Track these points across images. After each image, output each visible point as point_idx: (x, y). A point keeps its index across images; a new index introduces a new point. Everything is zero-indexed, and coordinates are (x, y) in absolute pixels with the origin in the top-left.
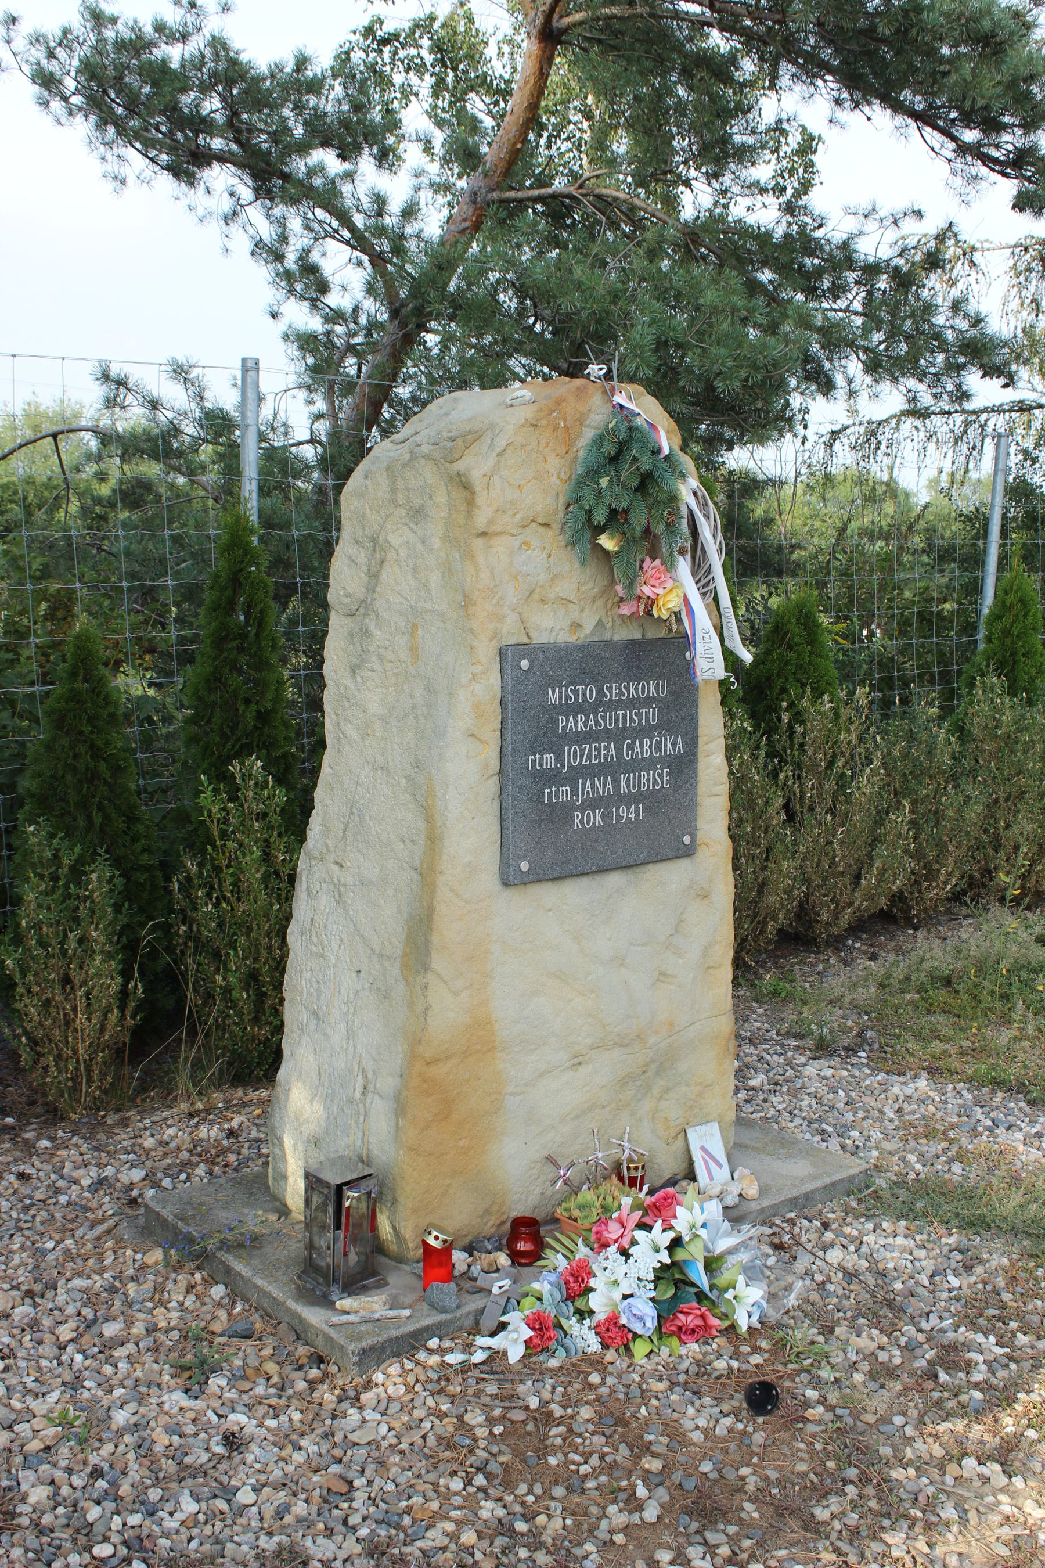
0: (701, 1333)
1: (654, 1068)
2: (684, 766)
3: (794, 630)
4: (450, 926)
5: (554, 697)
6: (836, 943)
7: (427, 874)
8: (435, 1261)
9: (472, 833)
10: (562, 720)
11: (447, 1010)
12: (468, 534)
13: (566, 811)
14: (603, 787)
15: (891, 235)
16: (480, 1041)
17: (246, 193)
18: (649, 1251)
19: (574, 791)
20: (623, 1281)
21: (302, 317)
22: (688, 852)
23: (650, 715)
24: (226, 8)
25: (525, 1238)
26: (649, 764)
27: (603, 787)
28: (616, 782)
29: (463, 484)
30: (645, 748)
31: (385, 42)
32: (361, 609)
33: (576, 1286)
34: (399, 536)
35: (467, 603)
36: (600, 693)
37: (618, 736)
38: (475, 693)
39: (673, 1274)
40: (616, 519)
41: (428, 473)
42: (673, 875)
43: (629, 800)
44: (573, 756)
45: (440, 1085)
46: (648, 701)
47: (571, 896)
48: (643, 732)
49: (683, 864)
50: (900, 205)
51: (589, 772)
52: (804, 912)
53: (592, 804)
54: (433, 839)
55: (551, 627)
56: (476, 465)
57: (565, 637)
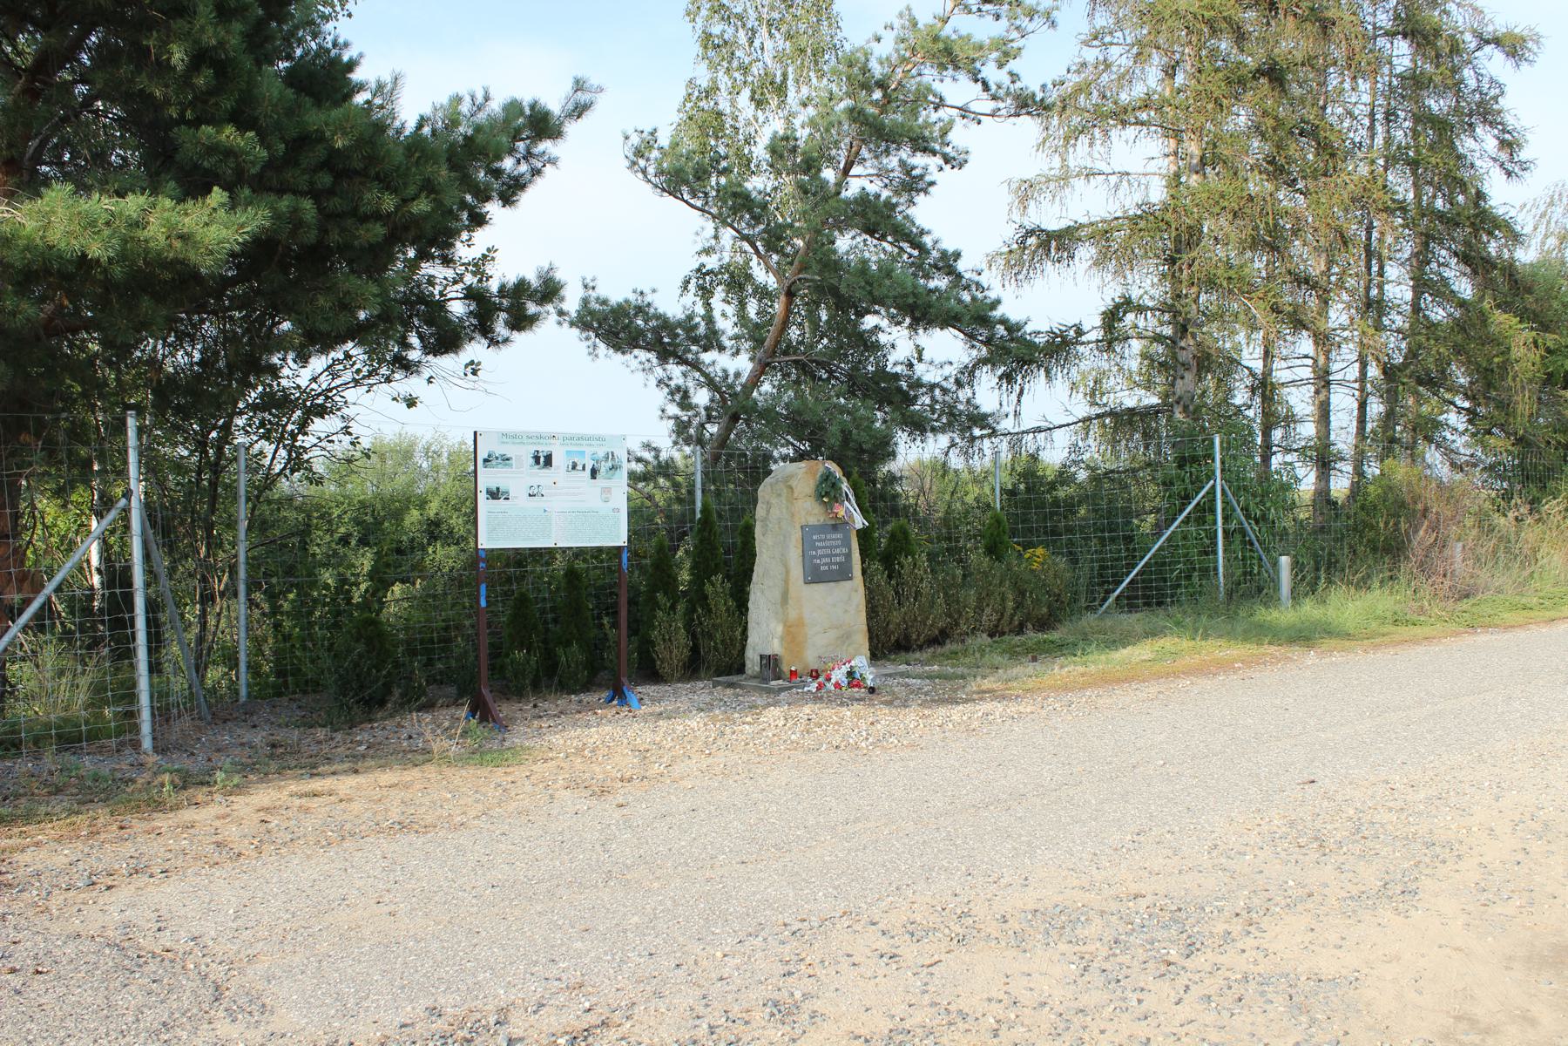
0: (858, 686)
1: (846, 637)
2: (848, 556)
3: (900, 536)
4: (792, 593)
6: (920, 648)
7: (786, 581)
8: (794, 674)
9: (797, 572)
11: (793, 614)
12: (792, 498)
14: (827, 560)
15: (940, 372)
16: (800, 623)
17: (655, 361)
18: (845, 669)
20: (839, 675)
21: (673, 410)
24: (654, 291)
25: (815, 675)
27: (827, 560)
29: (791, 488)
31: (708, 273)
32: (765, 520)
33: (829, 679)
34: (774, 501)
35: (793, 515)
37: (830, 547)
38: (796, 535)
39: (850, 674)
40: (827, 494)
41: (781, 485)
42: (847, 584)
45: (793, 634)
47: (820, 588)
50: (943, 359)
52: (907, 637)
54: (787, 572)
55: (813, 521)
56: (794, 483)
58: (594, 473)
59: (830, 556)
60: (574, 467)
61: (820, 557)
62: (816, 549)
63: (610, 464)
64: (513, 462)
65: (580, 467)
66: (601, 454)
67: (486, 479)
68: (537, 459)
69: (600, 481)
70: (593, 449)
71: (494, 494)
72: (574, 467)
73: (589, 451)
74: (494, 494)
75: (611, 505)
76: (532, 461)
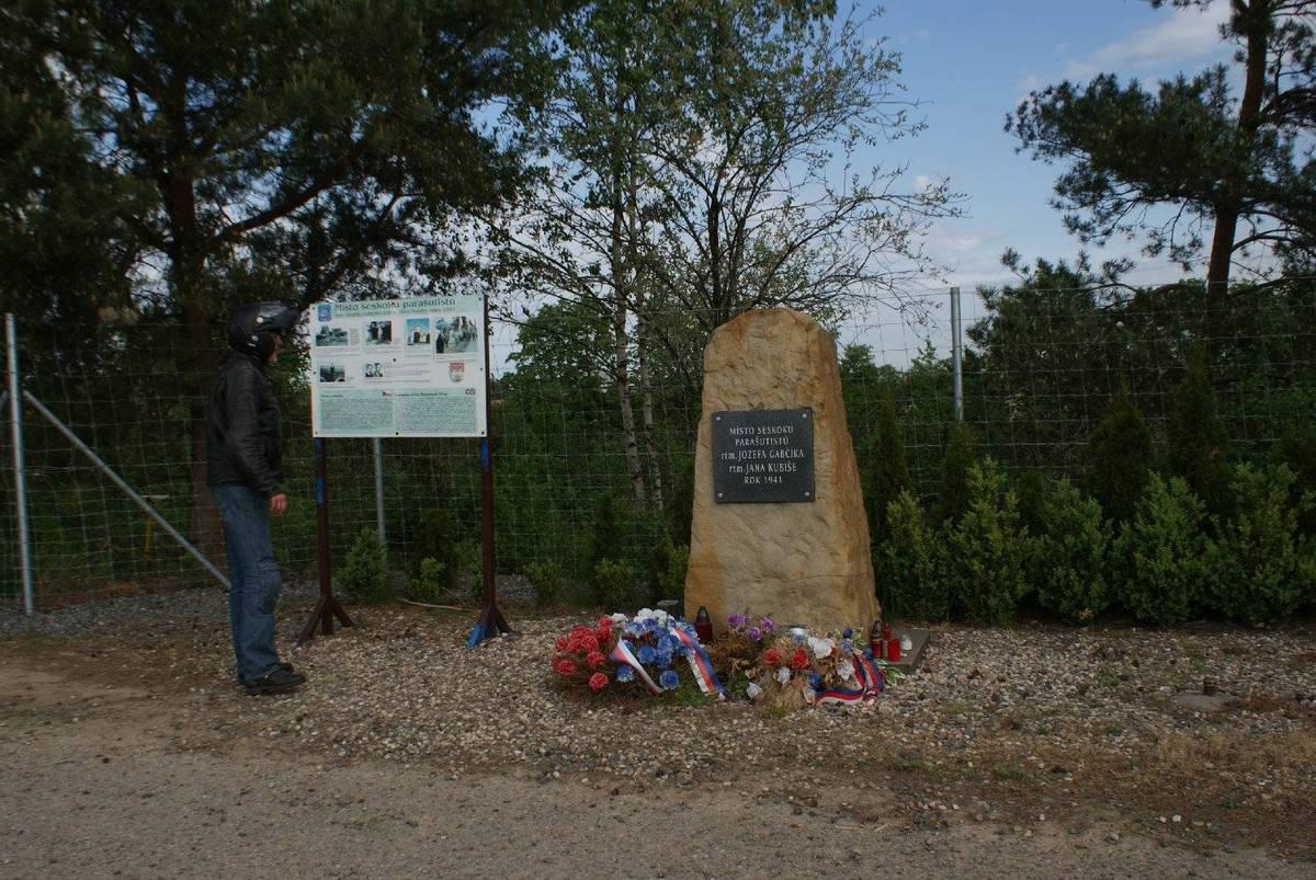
5: (733, 431)
10: (737, 441)
13: (741, 476)
19: (744, 468)
22: (811, 499)
23: (785, 441)
26: (785, 460)
28: (766, 467)
30: (782, 454)
36: (756, 430)
37: (767, 448)
43: (773, 474)
44: (742, 455)
46: (783, 435)
48: (780, 447)
49: (809, 505)
51: (754, 462)
53: (756, 474)
57: (748, 409)
58: (441, 345)
59: (765, 462)
60: (417, 336)
61: (744, 463)
62: (736, 450)
63: (460, 333)
64: (349, 337)
65: (423, 339)
66: (449, 319)
67: (319, 358)
68: (373, 331)
69: (450, 357)
70: (439, 316)
71: (329, 375)
72: (417, 336)
73: (433, 317)
74: (329, 375)
75: (466, 383)
76: (368, 335)
